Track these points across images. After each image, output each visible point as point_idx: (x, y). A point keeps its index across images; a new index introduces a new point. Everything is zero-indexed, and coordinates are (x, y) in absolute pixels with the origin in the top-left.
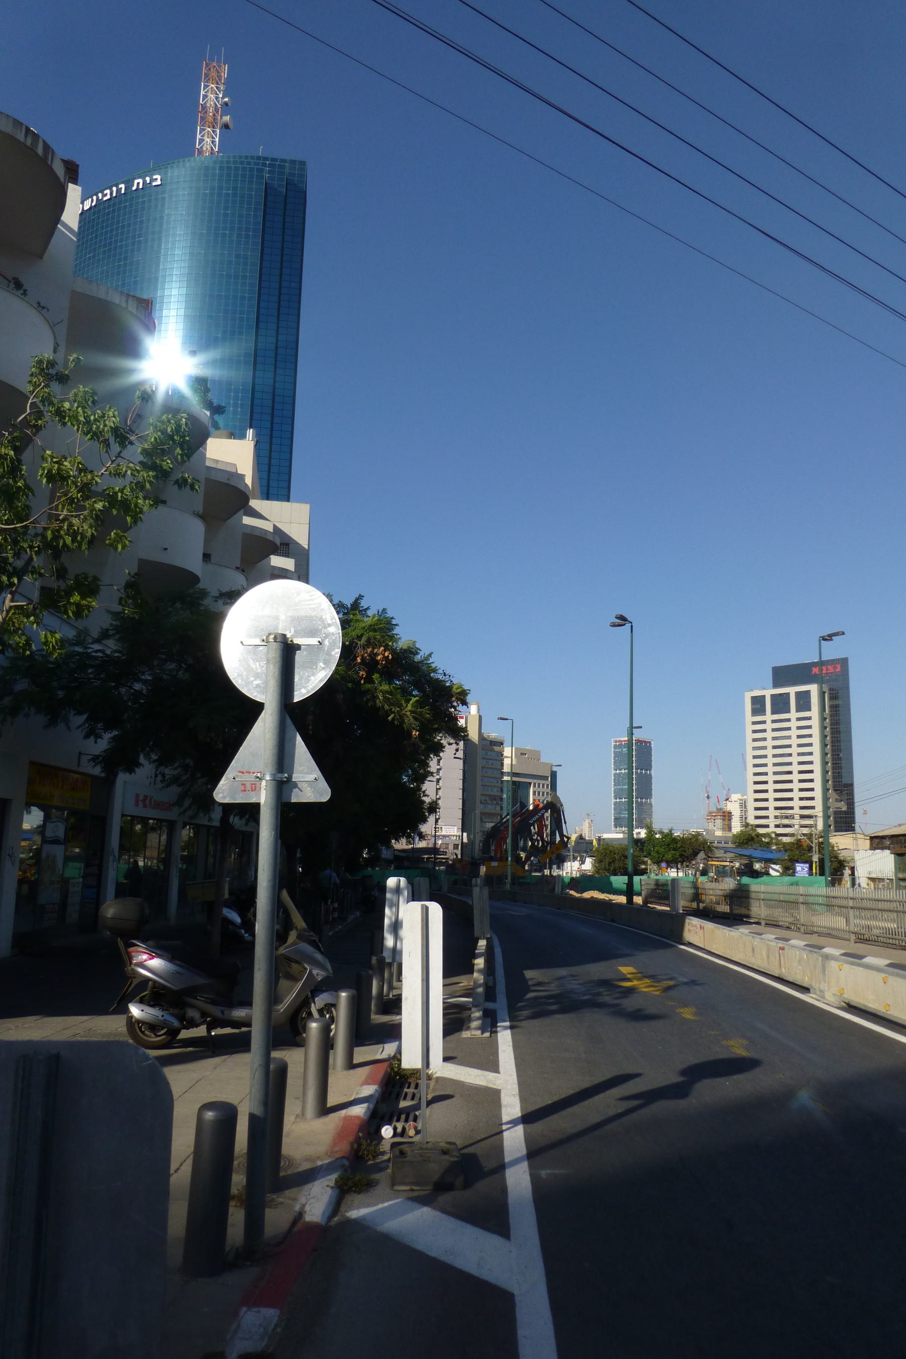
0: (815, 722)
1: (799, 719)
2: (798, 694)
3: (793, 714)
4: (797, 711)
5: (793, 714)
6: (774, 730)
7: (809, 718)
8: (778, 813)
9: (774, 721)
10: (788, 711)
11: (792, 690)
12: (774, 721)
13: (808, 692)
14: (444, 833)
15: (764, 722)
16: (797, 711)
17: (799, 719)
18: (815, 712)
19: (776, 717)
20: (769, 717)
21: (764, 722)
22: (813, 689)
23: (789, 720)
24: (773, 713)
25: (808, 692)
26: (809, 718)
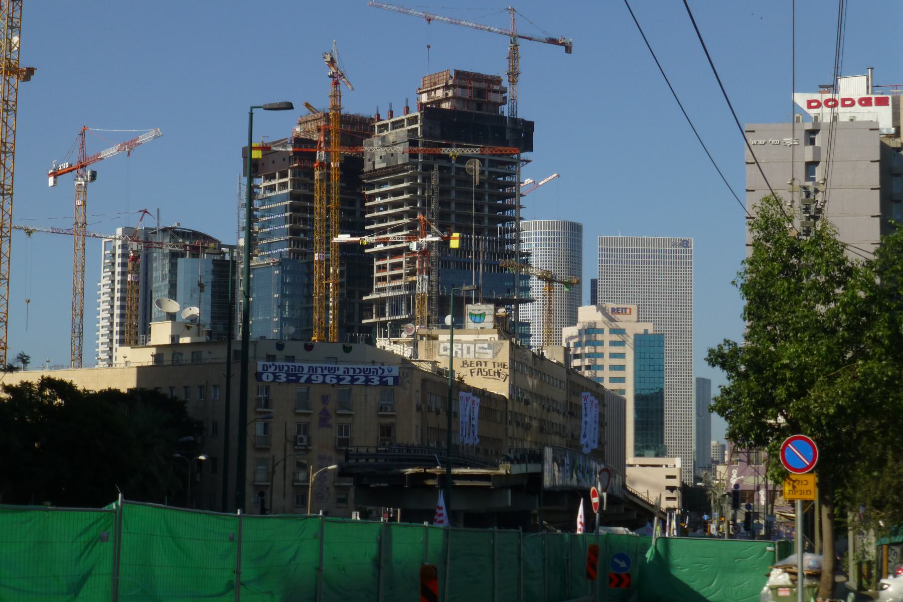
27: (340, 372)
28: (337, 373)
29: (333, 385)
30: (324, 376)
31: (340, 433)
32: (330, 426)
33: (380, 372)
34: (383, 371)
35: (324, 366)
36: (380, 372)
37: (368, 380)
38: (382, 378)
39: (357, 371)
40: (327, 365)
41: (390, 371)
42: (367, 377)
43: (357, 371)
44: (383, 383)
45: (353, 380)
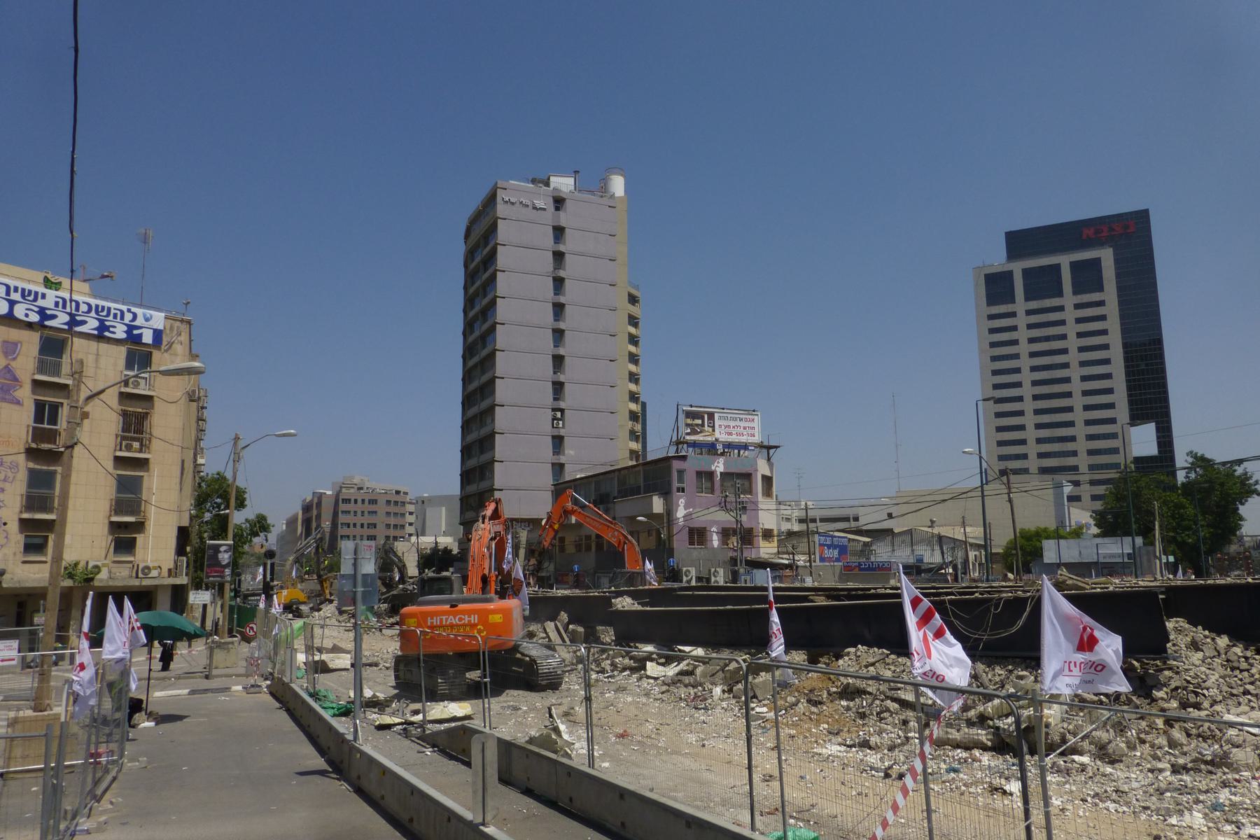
0: (1112, 308)
2: (1075, 266)
4: (1075, 293)
6: (1030, 327)
7: (1101, 303)
8: (1071, 461)
9: (1029, 313)
10: (1060, 294)
11: (1064, 261)
12: (1029, 313)
13: (1096, 263)
14: (721, 435)
15: (1013, 315)
16: (1075, 293)
18: (1110, 293)
19: (1034, 305)
21: (1013, 315)
23: (1061, 308)
25: (1096, 263)
26: (1101, 303)
27: (48, 303)
28: (40, 302)
29: (30, 326)
30: (12, 303)
31: (39, 417)
32: (18, 403)
33: (128, 317)
34: (135, 317)
35: (12, 283)
36: (128, 317)
37: (103, 327)
38: (131, 328)
39: (84, 308)
40: (21, 285)
41: (147, 320)
42: (101, 322)
43: (84, 308)
44: (133, 338)
45: (73, 322)
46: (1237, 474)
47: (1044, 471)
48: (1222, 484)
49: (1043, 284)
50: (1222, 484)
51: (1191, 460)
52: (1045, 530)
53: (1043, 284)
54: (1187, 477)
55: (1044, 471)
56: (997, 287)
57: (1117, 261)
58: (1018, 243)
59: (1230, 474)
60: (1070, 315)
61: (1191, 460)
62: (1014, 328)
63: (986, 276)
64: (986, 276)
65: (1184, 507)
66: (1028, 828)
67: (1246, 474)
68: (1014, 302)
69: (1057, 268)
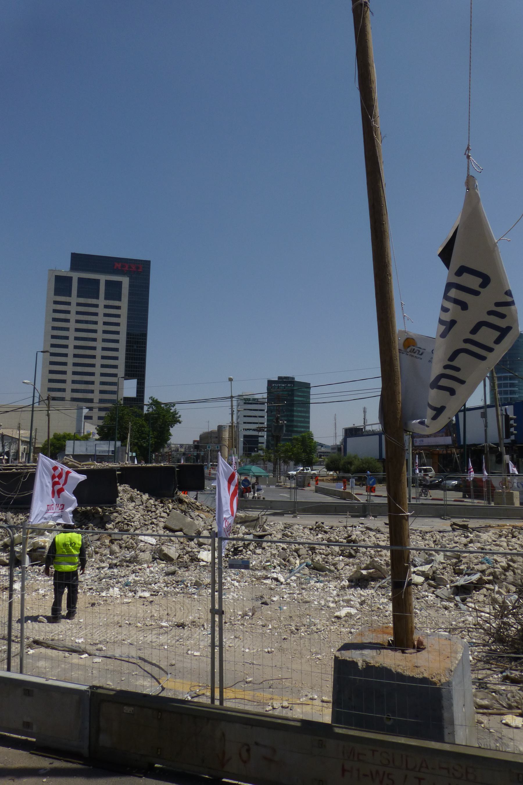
0: (124, 312)
1: (106, 307)
2: (108, 282)
3: (102, 301)
5: (102, 301)
6: (78, 313)
7: (118, 308)
8: (89, 396)
10: (97, 297)
11: (103, 278)
12: (78, 304)
13: (120, 284)
17: (106, 307)
19: (82, 300)
20: (74, 299)
21: (69, 304)
22: (125, 281)
23: (96, 306)
24: (79, 296)
25: (120, 284)
26: (118, 308)
46: (171, 411)
47: (74, 400)
48: (164, 416)
49: (88, 289)
50: (164, 416)
51: (151, 401)
52: (69, 435)
53: (88, 289)
54: (148, 411)
55: (74, 400)
56: (62, 285)
57: (131, 286)
58: (79, 261)
59: (168, 411)
60: (101, 310)
61: (151, 401)
62: (68, 312)
63: (56, 276)
64: (56, 276)
65: (144, 427)
66: (10, 605)
67: (175, 412)
68: (70, 296)
69: (97, 282)
